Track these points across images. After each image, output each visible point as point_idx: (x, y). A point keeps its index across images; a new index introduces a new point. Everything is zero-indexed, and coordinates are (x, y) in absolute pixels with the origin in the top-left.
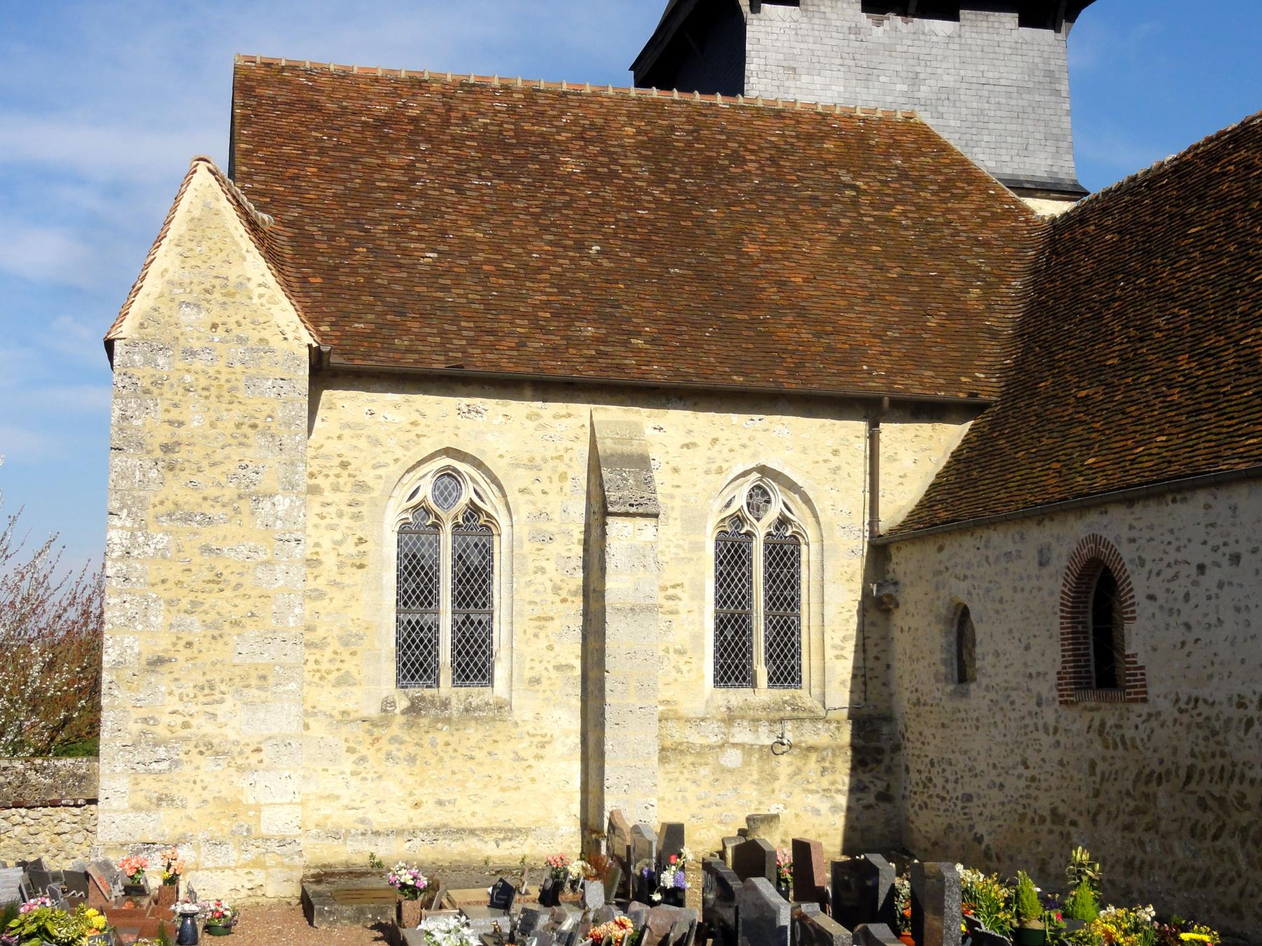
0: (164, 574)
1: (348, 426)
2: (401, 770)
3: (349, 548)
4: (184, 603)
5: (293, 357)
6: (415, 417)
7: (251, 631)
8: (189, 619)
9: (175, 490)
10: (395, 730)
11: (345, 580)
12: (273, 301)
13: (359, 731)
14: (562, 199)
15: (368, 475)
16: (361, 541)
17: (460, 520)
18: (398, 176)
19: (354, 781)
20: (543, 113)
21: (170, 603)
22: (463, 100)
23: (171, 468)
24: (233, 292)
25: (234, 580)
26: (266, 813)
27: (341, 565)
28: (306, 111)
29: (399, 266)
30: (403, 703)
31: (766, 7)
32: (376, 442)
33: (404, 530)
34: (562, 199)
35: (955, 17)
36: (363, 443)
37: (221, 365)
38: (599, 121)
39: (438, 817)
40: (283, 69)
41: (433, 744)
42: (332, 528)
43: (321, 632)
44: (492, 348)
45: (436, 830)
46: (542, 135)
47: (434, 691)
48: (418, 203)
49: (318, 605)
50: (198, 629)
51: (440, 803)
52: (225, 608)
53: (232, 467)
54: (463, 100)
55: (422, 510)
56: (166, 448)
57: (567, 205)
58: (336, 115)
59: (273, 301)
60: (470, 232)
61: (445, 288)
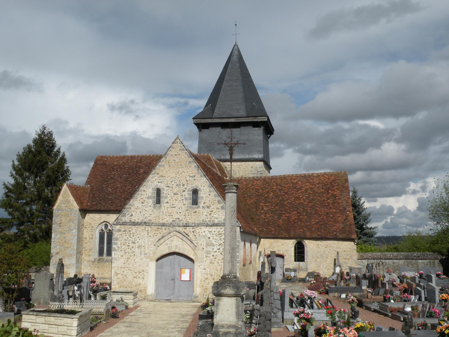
0: (59, 241)
1: (91, 218)
2: (96, 269)
3: (91, 236)
4: (61, 245)
5: (76, 210)
6: (100, 216)
7: (70, 249)
8: (62, 247)
9: (61, 229)
10: (96, 263)
11: (90, 241)
12: (74, 202)
13: (91, 263)
14: (136, 178)
15: (93, 225)
16: (92, 235)
17: (108, 231)
18: (112, 176)
19: (90, 270)
20: (142, 161)
21: (59, 245)
22: (130, 160)
23: (60, 226)
24: (68, 201)
25: (67, 242)
26: (71, 274)
27: (89, 239)
28: (103, 165)
29: (105, 192)
30: (98, 259)
31: (202, 130)
32: (95, 220)
33: (100, 232)
34: (136, 178)
35: (240, 128)
36: (93, 221)
37: (67, 212)
38: (150, 162)
39: (102, 276)
40: (103, 157)
41: (101, 265)
42: (88, 233)
43: (86, 248)
44: (112, 206)
45: (101, 278)
46: (140, 166)
47: (102, 257)
48: (113, 181)
49: (86, 245)
50: (63, 248)
51: (102, 274)
52: (66, 245)
53: (68, 226)
54: (130, 160)
55: (102, 230)
56: (60, 224)
57: (137, 179)
58: (108, 165)
59: (74, 202)
60: (118, 185)
61: (110, 196)
